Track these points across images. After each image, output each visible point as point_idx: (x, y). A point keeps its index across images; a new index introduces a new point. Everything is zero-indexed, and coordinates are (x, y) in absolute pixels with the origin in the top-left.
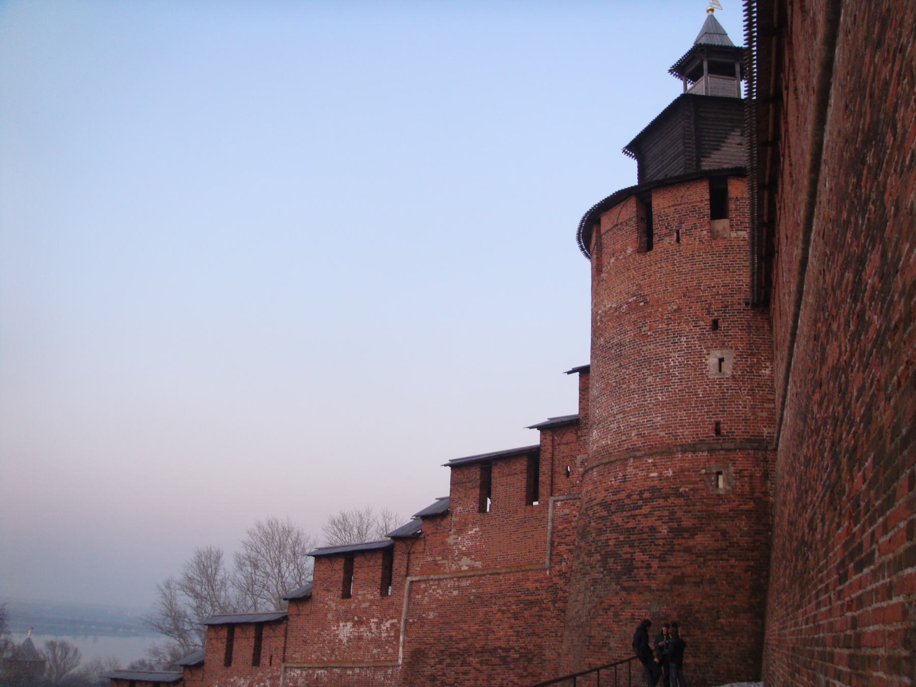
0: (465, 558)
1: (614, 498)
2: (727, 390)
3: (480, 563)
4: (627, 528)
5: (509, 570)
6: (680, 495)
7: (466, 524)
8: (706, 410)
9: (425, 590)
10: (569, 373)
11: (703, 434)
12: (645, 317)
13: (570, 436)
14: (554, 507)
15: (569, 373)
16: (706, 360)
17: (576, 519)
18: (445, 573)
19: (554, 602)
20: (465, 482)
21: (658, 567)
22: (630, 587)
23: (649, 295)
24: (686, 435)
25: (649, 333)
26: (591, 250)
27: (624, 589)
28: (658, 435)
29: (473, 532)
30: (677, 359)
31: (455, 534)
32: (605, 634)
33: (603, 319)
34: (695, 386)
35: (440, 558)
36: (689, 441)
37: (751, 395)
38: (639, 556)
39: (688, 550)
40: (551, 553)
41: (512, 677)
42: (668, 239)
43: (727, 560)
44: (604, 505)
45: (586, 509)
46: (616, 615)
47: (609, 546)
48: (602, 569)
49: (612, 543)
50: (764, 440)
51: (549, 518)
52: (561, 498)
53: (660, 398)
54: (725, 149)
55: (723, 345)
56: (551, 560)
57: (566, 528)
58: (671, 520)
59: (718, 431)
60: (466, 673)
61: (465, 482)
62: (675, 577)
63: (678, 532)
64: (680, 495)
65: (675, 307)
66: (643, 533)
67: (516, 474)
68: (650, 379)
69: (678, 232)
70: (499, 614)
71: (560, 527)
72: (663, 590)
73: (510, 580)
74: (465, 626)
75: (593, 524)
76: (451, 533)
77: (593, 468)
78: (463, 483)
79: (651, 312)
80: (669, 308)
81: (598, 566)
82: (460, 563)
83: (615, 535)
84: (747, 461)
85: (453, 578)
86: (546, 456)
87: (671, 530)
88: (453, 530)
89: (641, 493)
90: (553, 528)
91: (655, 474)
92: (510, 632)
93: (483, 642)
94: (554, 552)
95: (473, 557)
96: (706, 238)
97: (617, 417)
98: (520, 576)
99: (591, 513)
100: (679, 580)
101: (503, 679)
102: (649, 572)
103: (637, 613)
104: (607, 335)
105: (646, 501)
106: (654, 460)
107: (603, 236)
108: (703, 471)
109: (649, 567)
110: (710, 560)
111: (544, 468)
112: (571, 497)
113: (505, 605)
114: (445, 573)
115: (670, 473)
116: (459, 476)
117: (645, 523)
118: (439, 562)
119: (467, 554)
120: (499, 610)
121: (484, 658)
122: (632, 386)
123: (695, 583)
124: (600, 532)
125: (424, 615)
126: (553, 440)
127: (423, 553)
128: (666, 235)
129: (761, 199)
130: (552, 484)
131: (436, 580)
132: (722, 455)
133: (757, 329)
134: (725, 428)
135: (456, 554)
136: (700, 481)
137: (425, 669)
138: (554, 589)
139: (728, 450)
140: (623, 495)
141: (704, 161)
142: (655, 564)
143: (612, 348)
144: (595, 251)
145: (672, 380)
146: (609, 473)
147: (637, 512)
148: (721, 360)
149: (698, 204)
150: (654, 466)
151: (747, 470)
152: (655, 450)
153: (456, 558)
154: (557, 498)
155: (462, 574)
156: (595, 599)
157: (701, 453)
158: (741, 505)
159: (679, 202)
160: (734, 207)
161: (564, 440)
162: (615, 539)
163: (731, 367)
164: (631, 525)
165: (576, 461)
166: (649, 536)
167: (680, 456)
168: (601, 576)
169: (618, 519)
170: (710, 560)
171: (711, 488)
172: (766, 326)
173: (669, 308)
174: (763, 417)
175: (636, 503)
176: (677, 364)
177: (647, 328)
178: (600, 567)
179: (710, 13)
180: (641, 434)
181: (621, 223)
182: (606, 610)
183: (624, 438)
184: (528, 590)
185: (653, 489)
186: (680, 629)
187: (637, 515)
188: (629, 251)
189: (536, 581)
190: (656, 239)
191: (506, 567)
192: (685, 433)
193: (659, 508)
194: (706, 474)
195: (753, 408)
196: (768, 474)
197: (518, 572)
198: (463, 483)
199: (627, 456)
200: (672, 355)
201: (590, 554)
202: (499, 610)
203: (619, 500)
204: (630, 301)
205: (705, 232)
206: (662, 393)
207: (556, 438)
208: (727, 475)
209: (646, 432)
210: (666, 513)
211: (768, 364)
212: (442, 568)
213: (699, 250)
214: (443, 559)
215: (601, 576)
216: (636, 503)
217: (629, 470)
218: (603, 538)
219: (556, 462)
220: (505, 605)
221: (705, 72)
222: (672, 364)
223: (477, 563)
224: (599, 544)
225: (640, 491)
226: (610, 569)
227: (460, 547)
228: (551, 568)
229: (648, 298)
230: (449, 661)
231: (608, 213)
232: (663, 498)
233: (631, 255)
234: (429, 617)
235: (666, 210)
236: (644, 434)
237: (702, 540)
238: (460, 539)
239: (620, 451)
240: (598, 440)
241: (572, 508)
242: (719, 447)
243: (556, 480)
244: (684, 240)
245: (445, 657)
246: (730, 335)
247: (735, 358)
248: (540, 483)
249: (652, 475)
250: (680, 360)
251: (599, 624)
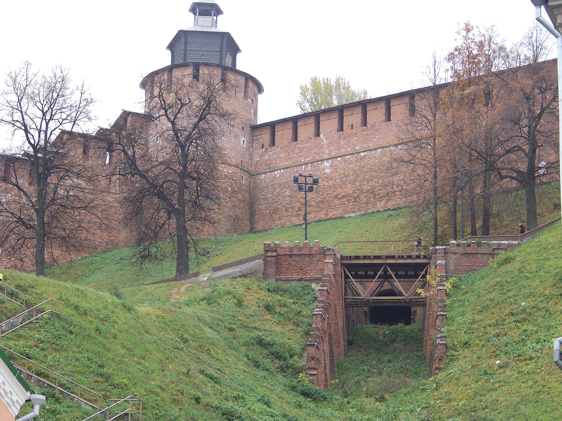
6: (234, 180)
63: (234, 191)
64: (234, 180)
109: (226, 200)
142: (227, 199)
185: (225, 175)
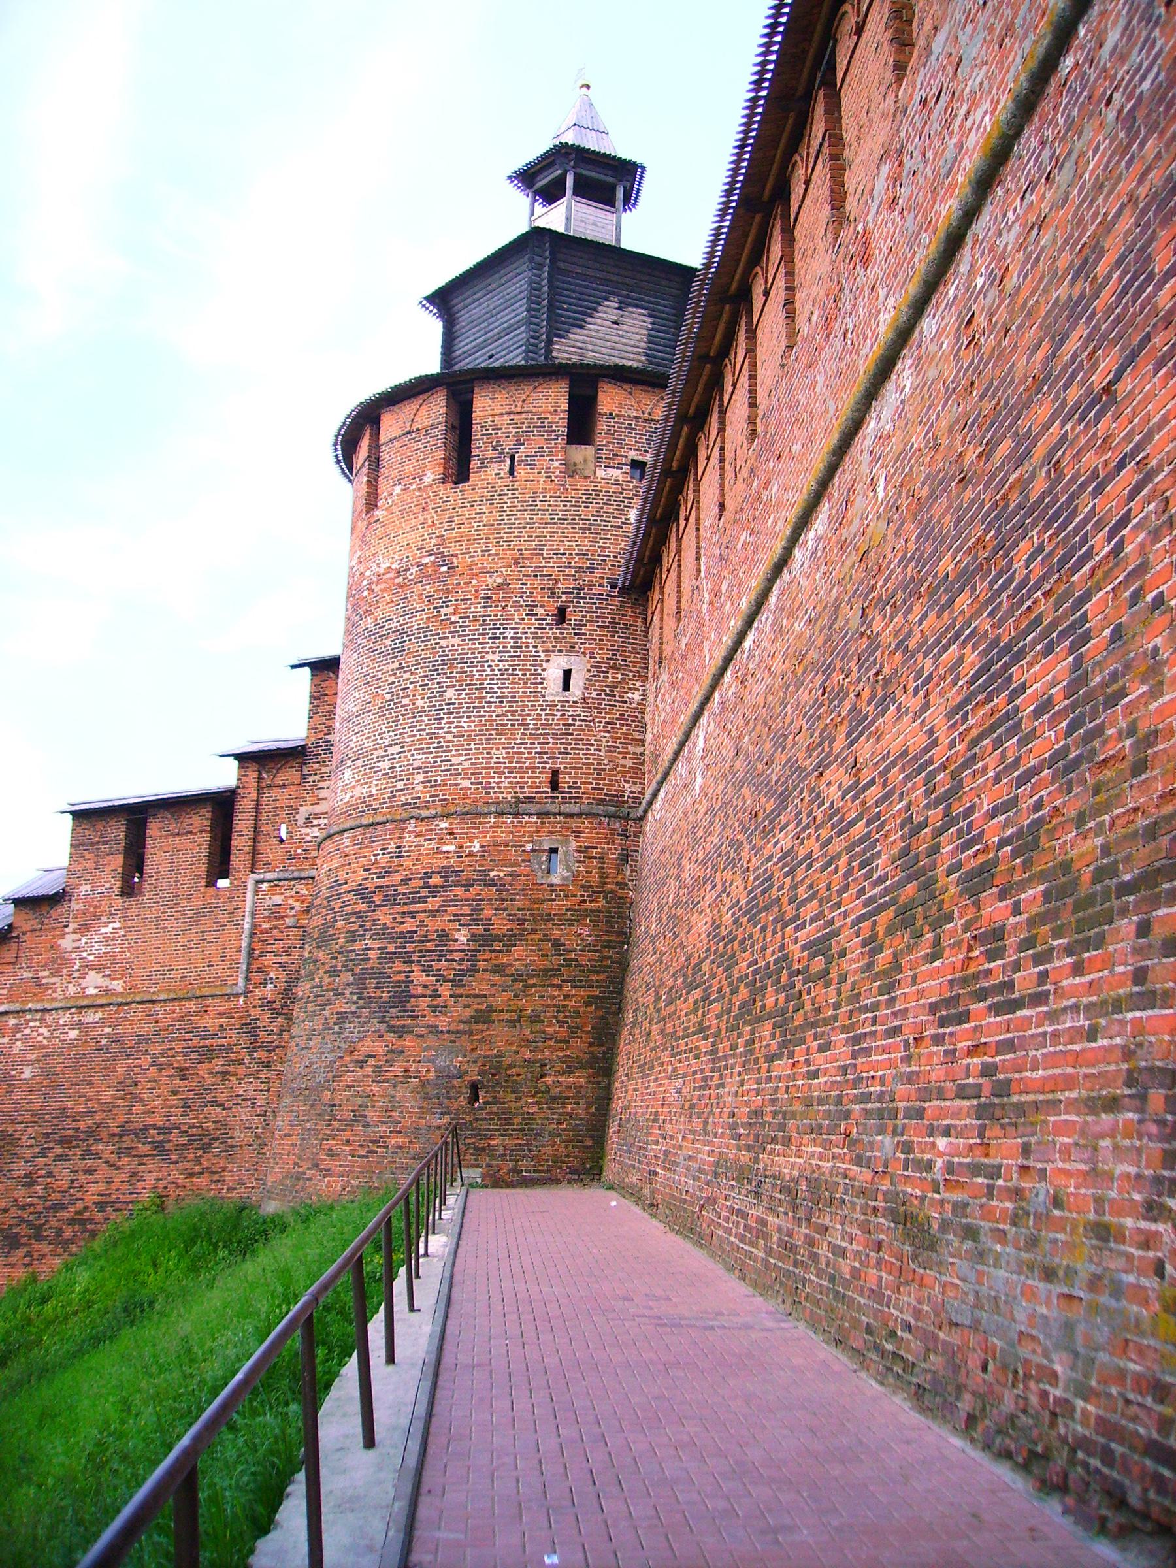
0: (92, 973)
1: (381, 882)
2: (574, 720)
3: (121, 982)
4: (402, 933)
5: (172, 996)
6: (492, 883)
7: (96, 916)
8: (538, 750)
9: (17, 1029)
10: (294, 667)
11: (531, 787)
12: (448, 591)
13: (289, 775)
14: (257, 892)
15: (294, 667)
16: (544, 670)
17: (293, 912)
18: (55, 1000)
19: (251, 1049)
20: (98, 843)
21: (451, 996)
22: (404, 1026)
23: (456, 555)
24: (504, 787)
25: (453, 619)
26: (357, 466)
27: (392, 1029)
28: (458, 784)
29: (109, 929)
30: (497, 665)
31: (74, 932)
32: (359, 1101)
33: (374, 587)
34: (523, 711)
35: (46, 973)
36: (509, 797)
37: (608, 732)
38: (419, 977)
39: (499, 970)
40: (248, 969)
41: (175, 1175)
42: (494, 468)
43: (559, 987)
44: (361, 892)
45: (329, 900)
46: (378, 1070)
47: (369, 959)
48: (355, 997)
49: (372, 955)
50: (624, 802)
51: (248, 909)
52: (269, 876)
53: (465, 725)
54: (591, 327)
55: (571, 650)
56: (247, 979)
57: (276, 927)
58: (475, 921)
59: (554, 784)
60: (89, 1171)
61: (98, 843)
62: (476, 1011)
63: (484, 941)
65: (500, 580)
66: (429, 941)
67: (191, 832)
68: (450, 693)
69: (512, 458)
70: (154, 1070)
71: (265, 926)
72: (457, 1032)
73: (174, 1012)
74: (90, 1092)
75: (340, 924)
76: (67, 930)
77: (343, 831)
78: (93, 844)
79: (458, 584)
80: (490, 581)
81: (347, 992)
82: (84, 983)
83: (376, 944)
84: (597, 833)
85: (70, 1008)
86: (245, 804)
87: (473, 938)
88: (72, 926)
89: (427, 876)
90: (254, 926)
91: (452, 848)
92: (173, 1100)
93: (122, 1119)
94: (254, 967)
95: (108, 972)
96: (558, 473)
97: (390, 750)
98: (192, 1005)
99: (337, 905)
100: (483, 1017)
101: (159, 1179)
102: (435, 1002)
103: (413, 1067)
104: (379, 613)
105: (434, 890)
106: (451, 824)
107: (383, 448)
108: (529, 847)
109: (435, 995)
110: (534, 986)
111: (242, 825)
112: (287, 875)
113: (162, 1055)
114: (55, 1000)
115: (476, 847)
116: (87, 833)
117: (433, 925)
118: (44, 981)
119: (97, 968)
120: (154, 1064)
121: (125, 1145)
122: (420, 703)
123: (508, 1021)
124: (353, 937)
125: (13, 1073)
126: (260, 779)
127: (14, 963)
128: (493, 460)
129: (675, 435)
130: (255, 852)
131: (37, 1011)
132: (560, 822)
133: (626, 627)
134: (565, 781)
135: (76, 967)
136: (523, 861)
137: (14, 1166)
138: (251, 1028)
139: (570, 815)
140: (395, 879)
141: (556, 343)
142: (445, 990)
143: (386, 636)
144: (365, 470)
145: (485, 697)
146: (373, 842)
147: (418, 907)
148: (567, 674)
149: (548, 415)
150: (451, 834)
151: (596, 848)
152: (453, 810)
153: (76, 975)
154: (262, 876)
155: (85, 1002)
156: (343, 1045)
157: (526, 818)
158: (585, 901)
159: (519, 409)
161: (278, 781)
162: (379, 948)
163: (581, 684)
164: (406, 928)
165: (297, 816)
166: (437, 946)
167: (493, 820)
168: (354, 1008)
169: (384, 916)
170: (534, 986)
171: (540, 874)
172: (639, 624)
173: (490, 581)
174: (624, 766)
175: (418, 893)
176: (496, 672)
177: (451, 610)
178: (351, 993)
180: (430, 782)
181: (418, 430)
182: (361, 1063)
183: (400, 785)
184: (205, 1029)
185: (446, 872)
186: (482, 1093)
187: (418, 912)
188: (429, 478)
189: (221, 1014)
190: (475, 464)
191: (169, 991)
192: (502, 785)
193: (455, 902)
194: (533, 850)
195: (611, 750)
196: (627, 856)
197: (190, 999)
198: (93, 844)
199: (405, 815)
200: (489, 657)
201: (333, 972)
202: (154, 1064)
203: (388, 886)
204: (425, 560)
206: (469, 717)
207: (265, 776)
208: (566, 853)
209: (439, 778)
210: (466, 910)
211: (638, 684)
212: (50, 992)
213: (545, 491)
214: (52, 975)
215: (354, 1008)
216: (418, 893)
217: (409, 838)
218: (359, 946)
219: (264, 817)
220: (162, 1055)
221: (569, 192)
222: (489, 672)
223: (115, 982)
224: (352, 956)
225: (426, 873)
226: (370, 997)
227: (84, 954)
228: (246, 994)
229: (455, 561)
230: (59, 1151)
231: (395, 408)
232: (462, 886)
233: (431, 486)
234: (23, 1076)
235: (497, 418)
236: (436, 781)
237: (523, 955)
238: (84, 940)
239: (392, 807)
240: (354, 787)
241: (288, 894)
242: (557, 811)
243: (262, 846)
244: (521, 472)
245: (51, 1145)
246: (584, 634)
247: (589, 671)
248: (233, 850)
249: (445, 848)
250: (501, 667)
251: (347, 1086)
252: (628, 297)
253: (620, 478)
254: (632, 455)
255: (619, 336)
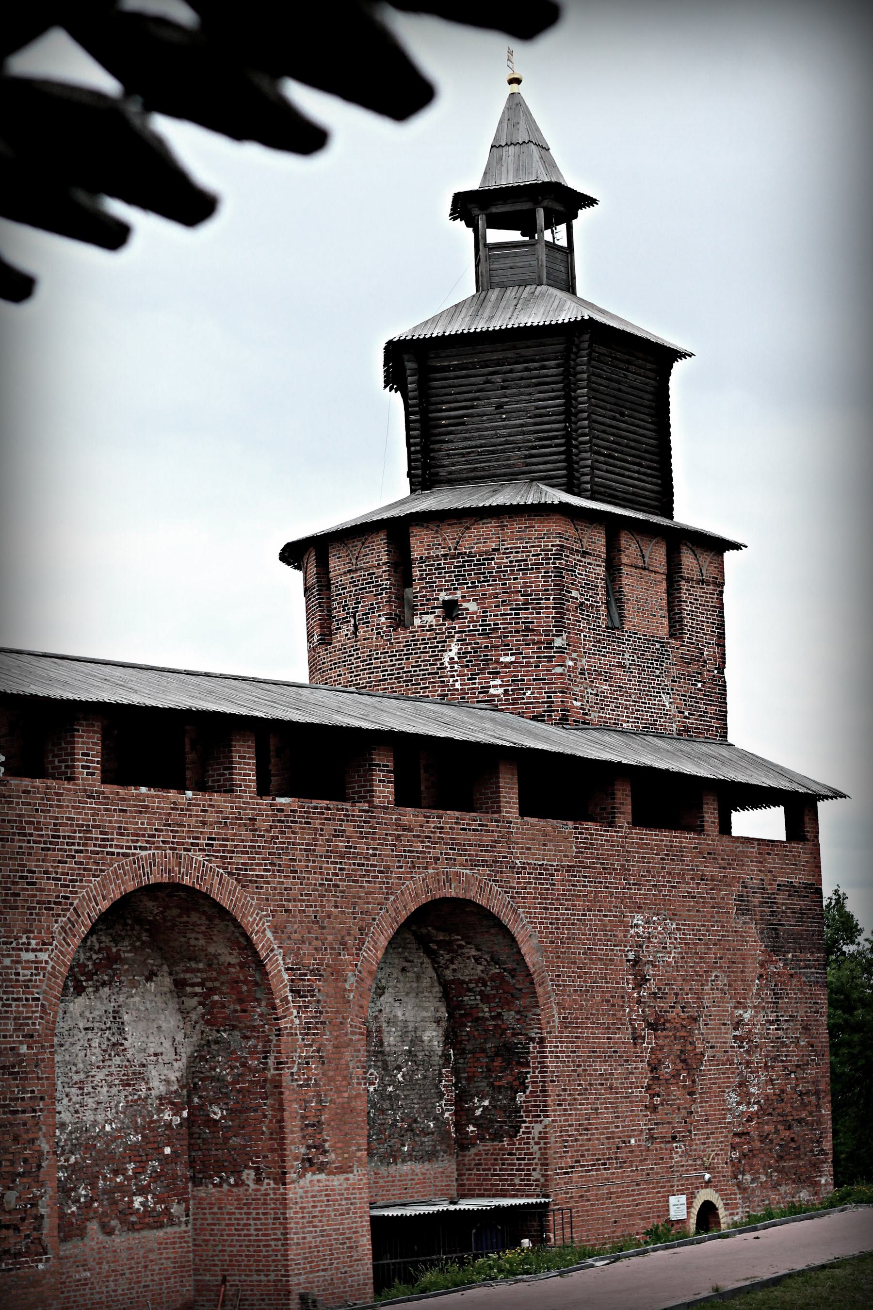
160: (418, 573)
179: (515, 88)
205: (383, 619)
252: (511, 371)
253: (434, 623)
254: (443, 596)
255: (504, 420)
